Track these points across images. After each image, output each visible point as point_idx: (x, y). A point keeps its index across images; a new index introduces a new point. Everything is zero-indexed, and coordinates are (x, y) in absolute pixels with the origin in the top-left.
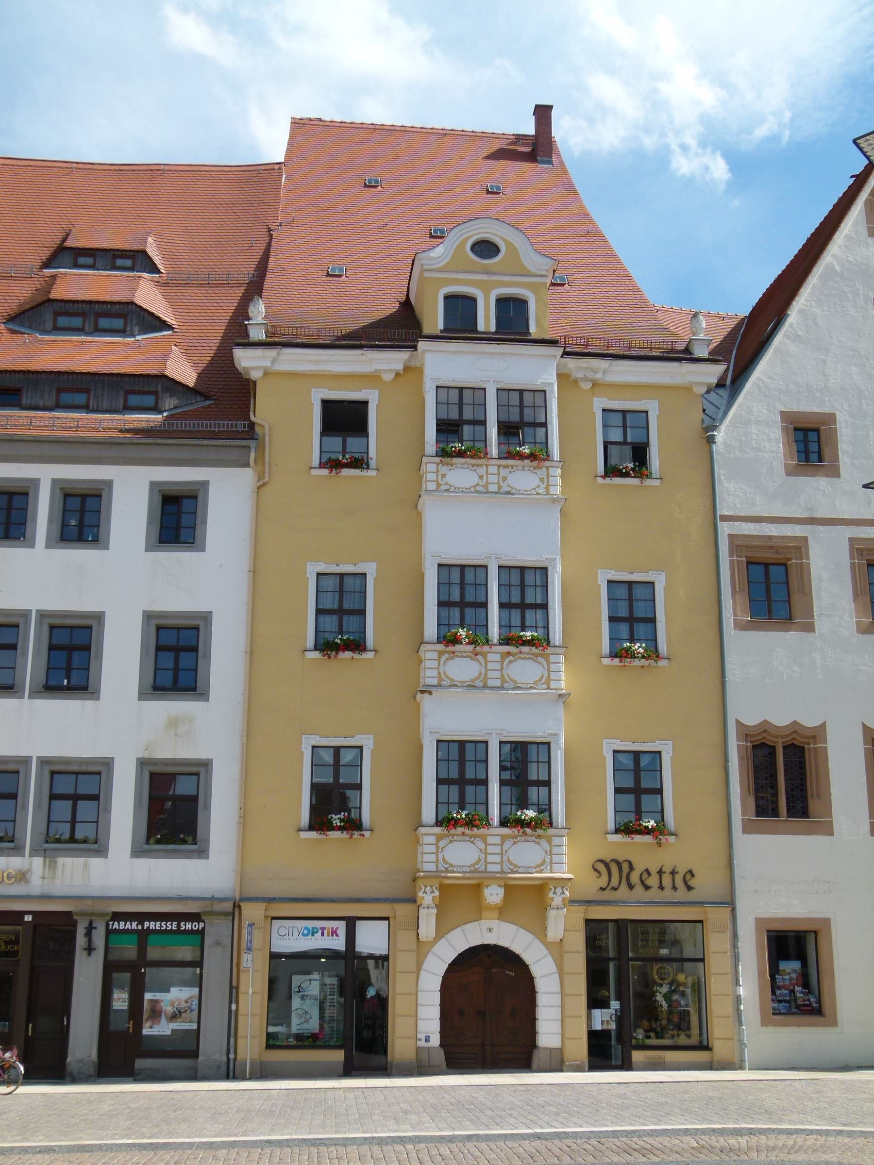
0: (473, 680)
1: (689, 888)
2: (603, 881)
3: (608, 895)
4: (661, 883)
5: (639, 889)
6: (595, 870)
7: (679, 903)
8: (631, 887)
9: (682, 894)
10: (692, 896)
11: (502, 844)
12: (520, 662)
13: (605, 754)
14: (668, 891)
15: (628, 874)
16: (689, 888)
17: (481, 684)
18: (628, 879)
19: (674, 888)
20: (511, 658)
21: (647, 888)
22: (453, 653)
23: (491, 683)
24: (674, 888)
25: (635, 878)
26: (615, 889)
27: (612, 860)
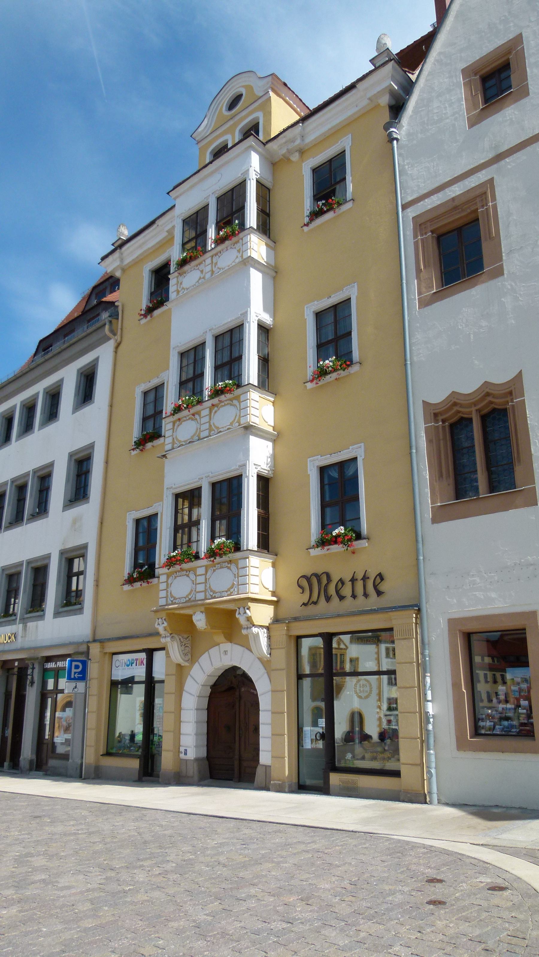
0: (192, 437)
1: (379, 593)
2: (305, 598)
3: (311, 610)
4: (353, 591)
5: (335, 599)
6: (299, 586)
7: (371, 610)
8: (328, 599)
9: (373, 601)
10: (383, 602)
11: (206, 574)
12: (221, 409)
13: (309, 472)
14: (361, 598)
15: (326, 586)
16: (379, 593)
17: (197, 438)
18: (326, 591)
19: (366, 595)
20: (216, 409)
21: (342, 598)
22: (179, 419)
23: (203, 435)
24: (366, 595)
25: (332, 590)
26: (315, 603)
27: (312, 575)
